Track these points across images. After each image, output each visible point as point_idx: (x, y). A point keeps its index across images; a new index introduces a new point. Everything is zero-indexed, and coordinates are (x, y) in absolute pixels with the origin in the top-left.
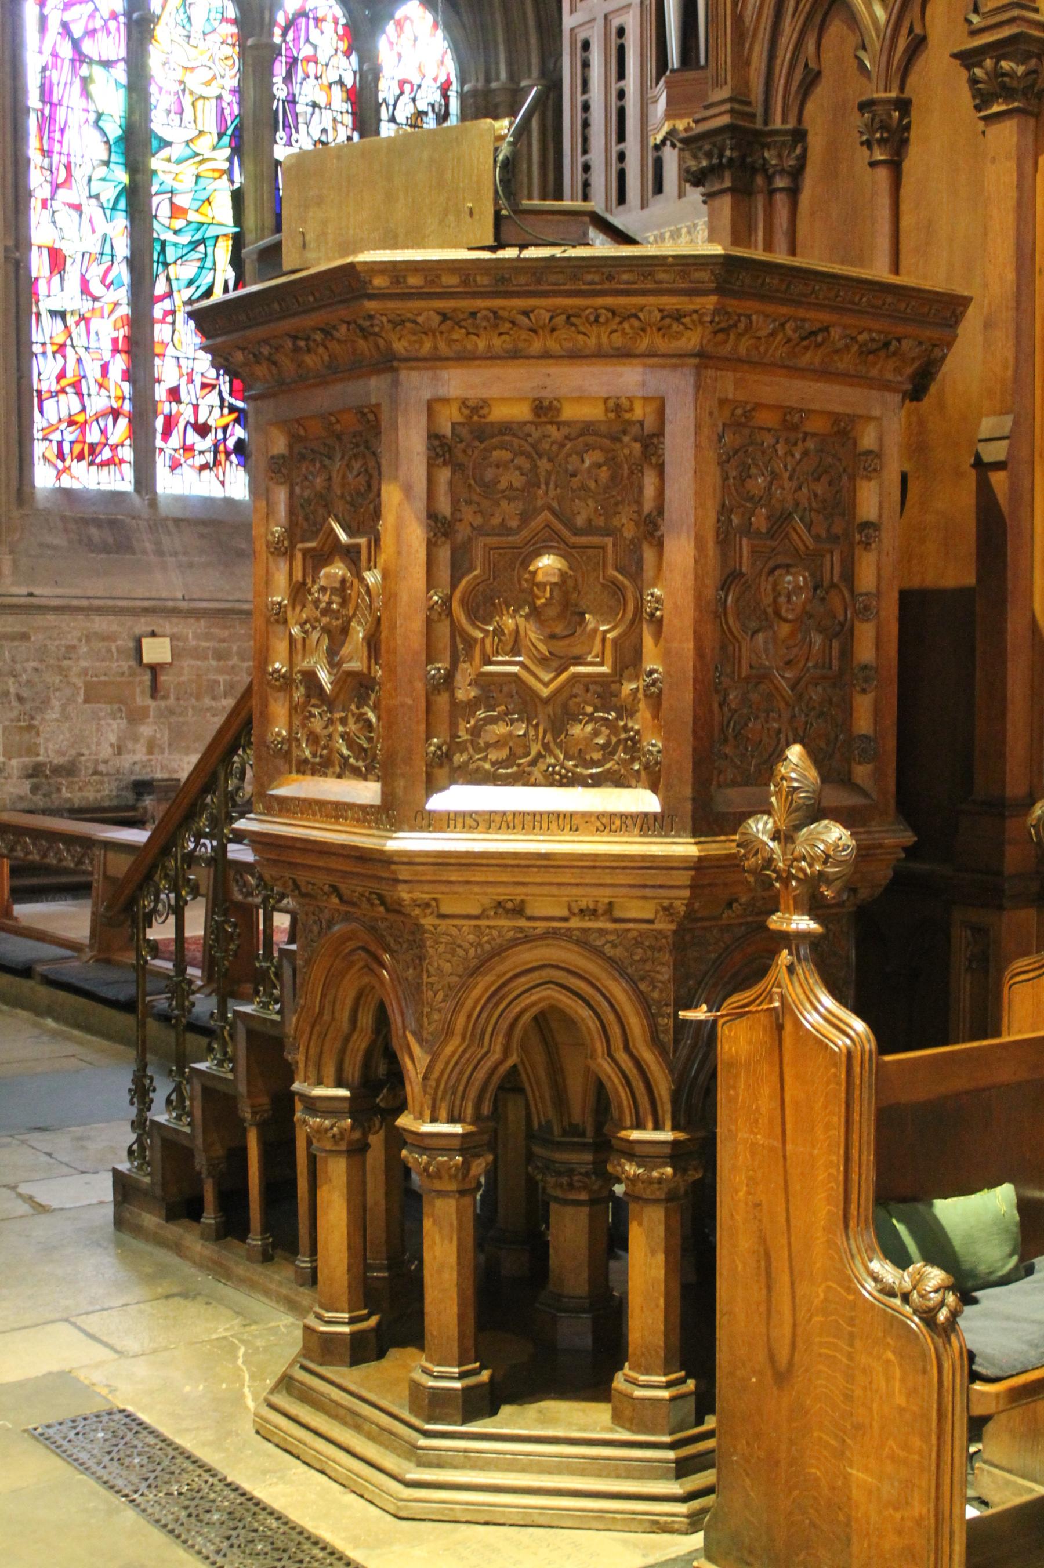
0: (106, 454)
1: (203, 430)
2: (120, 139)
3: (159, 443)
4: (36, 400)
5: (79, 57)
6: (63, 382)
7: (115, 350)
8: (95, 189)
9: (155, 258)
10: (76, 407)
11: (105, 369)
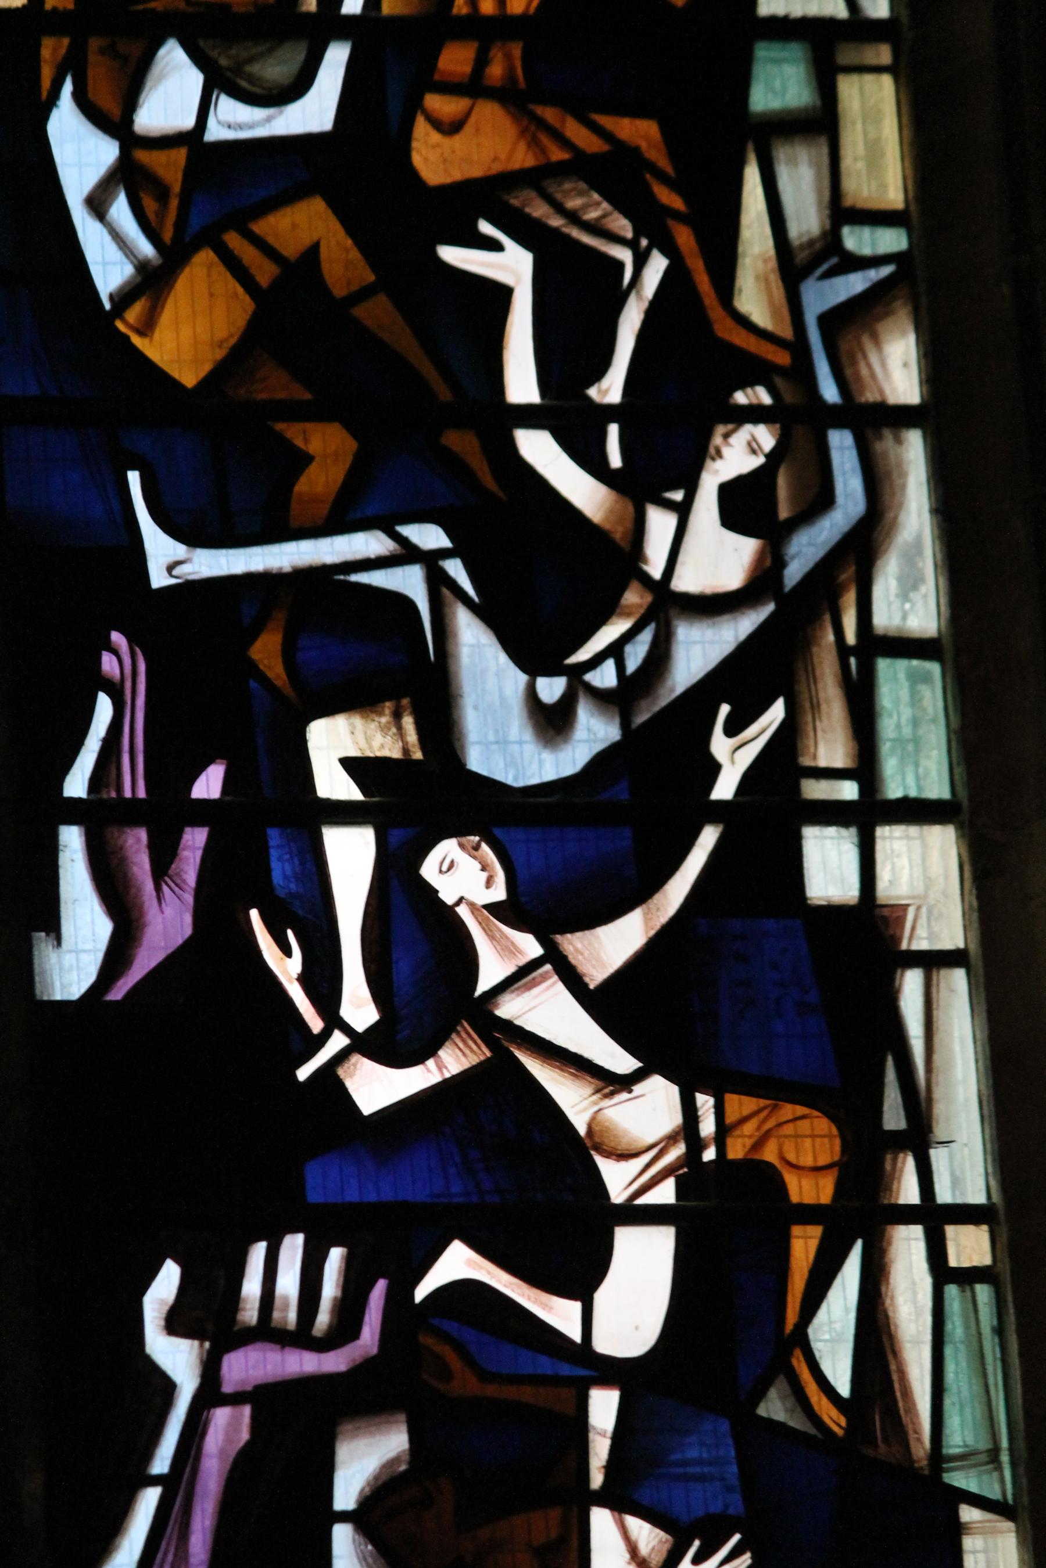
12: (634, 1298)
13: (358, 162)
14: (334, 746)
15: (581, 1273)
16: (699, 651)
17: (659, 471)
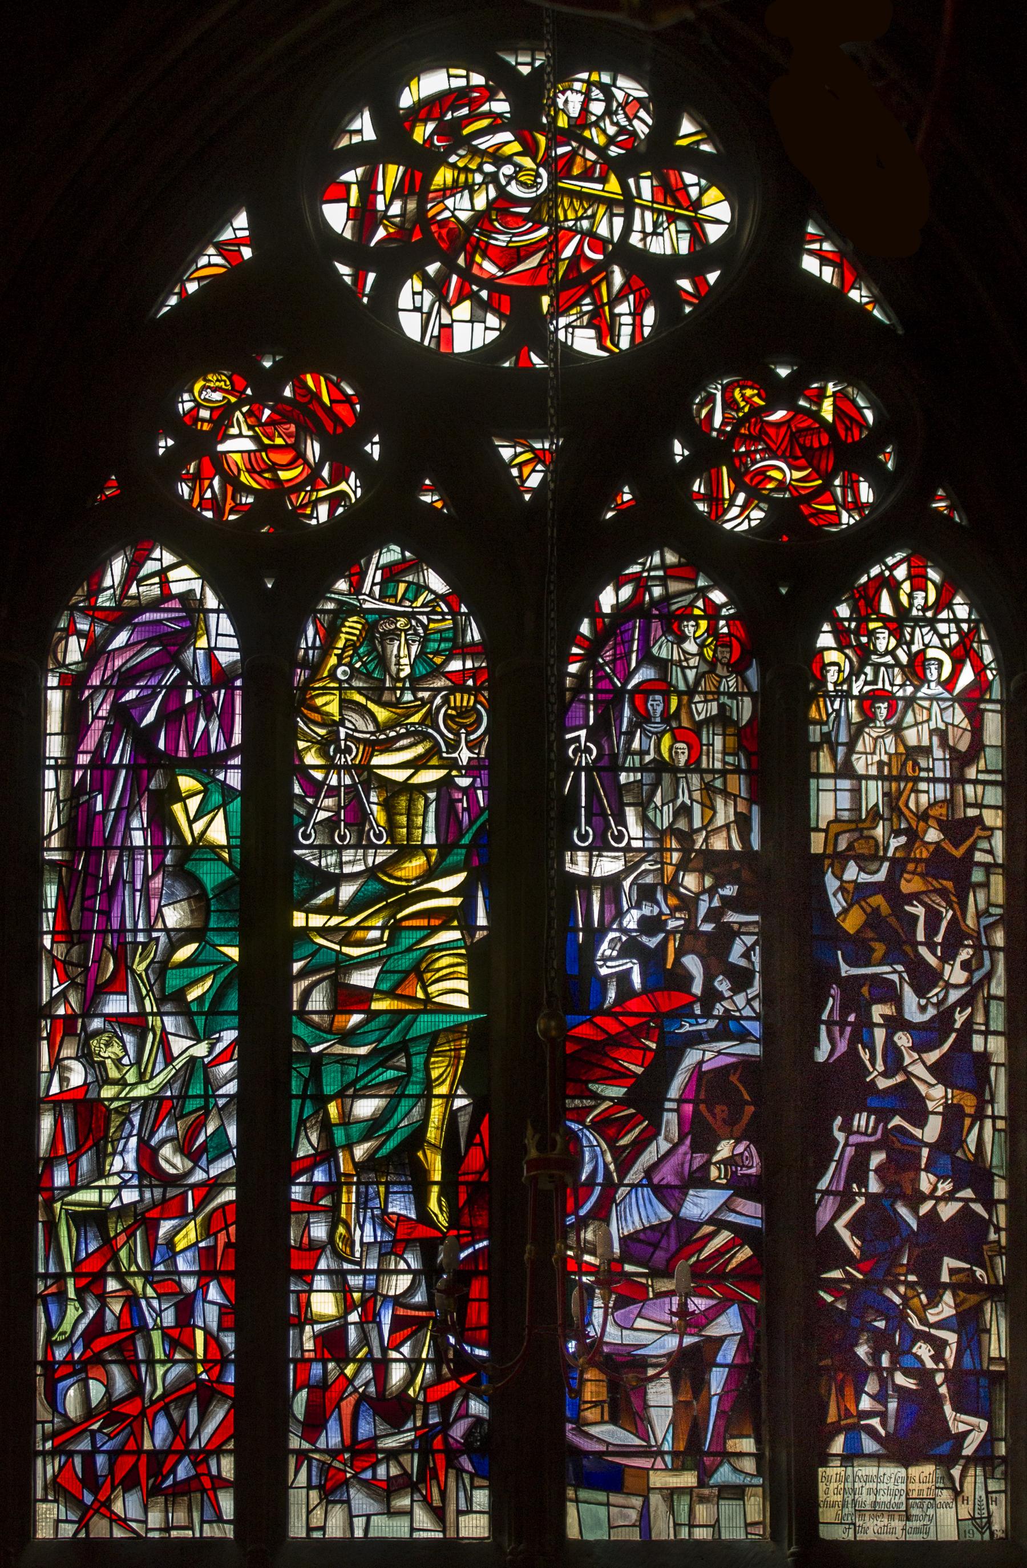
0: (184, 1470)
1: (393, 1408)
2: (224, 889)
3: (295, 1443)
4: (40, 1383)
5: (148, 760)
6: (99, 1344)
7: (204, 1276)
8: (174, 981)
9: (296, 1086)
10: (121, 1385)
11: (186, 1307)
12: (932, 1131)
13: (889, 888)
14: (878, 1011)
15: (921, 1124)
16: (954, 996)
17: (948, 956)
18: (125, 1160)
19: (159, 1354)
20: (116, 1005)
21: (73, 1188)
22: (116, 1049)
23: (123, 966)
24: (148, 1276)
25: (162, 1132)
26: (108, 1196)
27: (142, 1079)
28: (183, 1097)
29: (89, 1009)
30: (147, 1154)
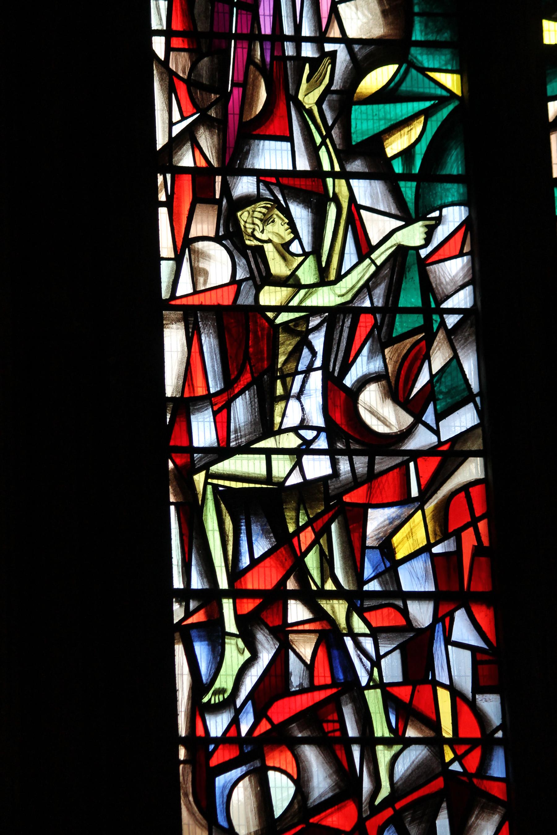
4: (185, 774)
6: (281, 711)
7: (446, 599)
10: (321, 781)
11: (418, 651)
18: (306, 405)
19: (381, 729)
20: (272, 156)
21: (222, 451)
22: (278, 230)
23: (283, 94)
24: (357, 600)
25: (363, 366)
26: (281, 466)
27: (323, 280)
28: (391, 309)
29: (233, 162)
30: (341, 400)
